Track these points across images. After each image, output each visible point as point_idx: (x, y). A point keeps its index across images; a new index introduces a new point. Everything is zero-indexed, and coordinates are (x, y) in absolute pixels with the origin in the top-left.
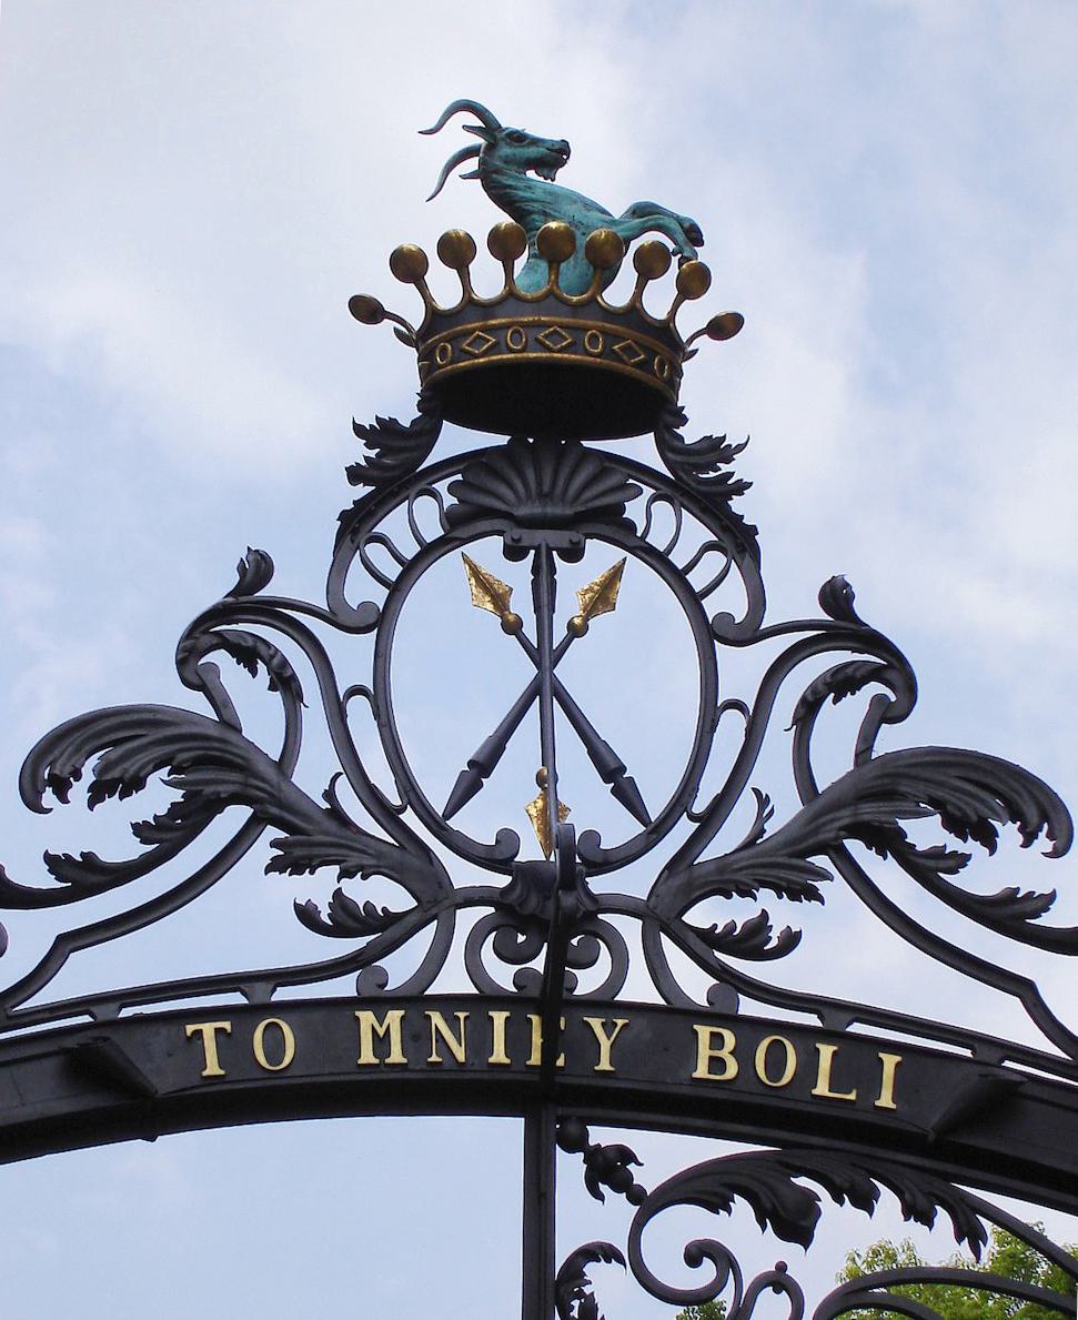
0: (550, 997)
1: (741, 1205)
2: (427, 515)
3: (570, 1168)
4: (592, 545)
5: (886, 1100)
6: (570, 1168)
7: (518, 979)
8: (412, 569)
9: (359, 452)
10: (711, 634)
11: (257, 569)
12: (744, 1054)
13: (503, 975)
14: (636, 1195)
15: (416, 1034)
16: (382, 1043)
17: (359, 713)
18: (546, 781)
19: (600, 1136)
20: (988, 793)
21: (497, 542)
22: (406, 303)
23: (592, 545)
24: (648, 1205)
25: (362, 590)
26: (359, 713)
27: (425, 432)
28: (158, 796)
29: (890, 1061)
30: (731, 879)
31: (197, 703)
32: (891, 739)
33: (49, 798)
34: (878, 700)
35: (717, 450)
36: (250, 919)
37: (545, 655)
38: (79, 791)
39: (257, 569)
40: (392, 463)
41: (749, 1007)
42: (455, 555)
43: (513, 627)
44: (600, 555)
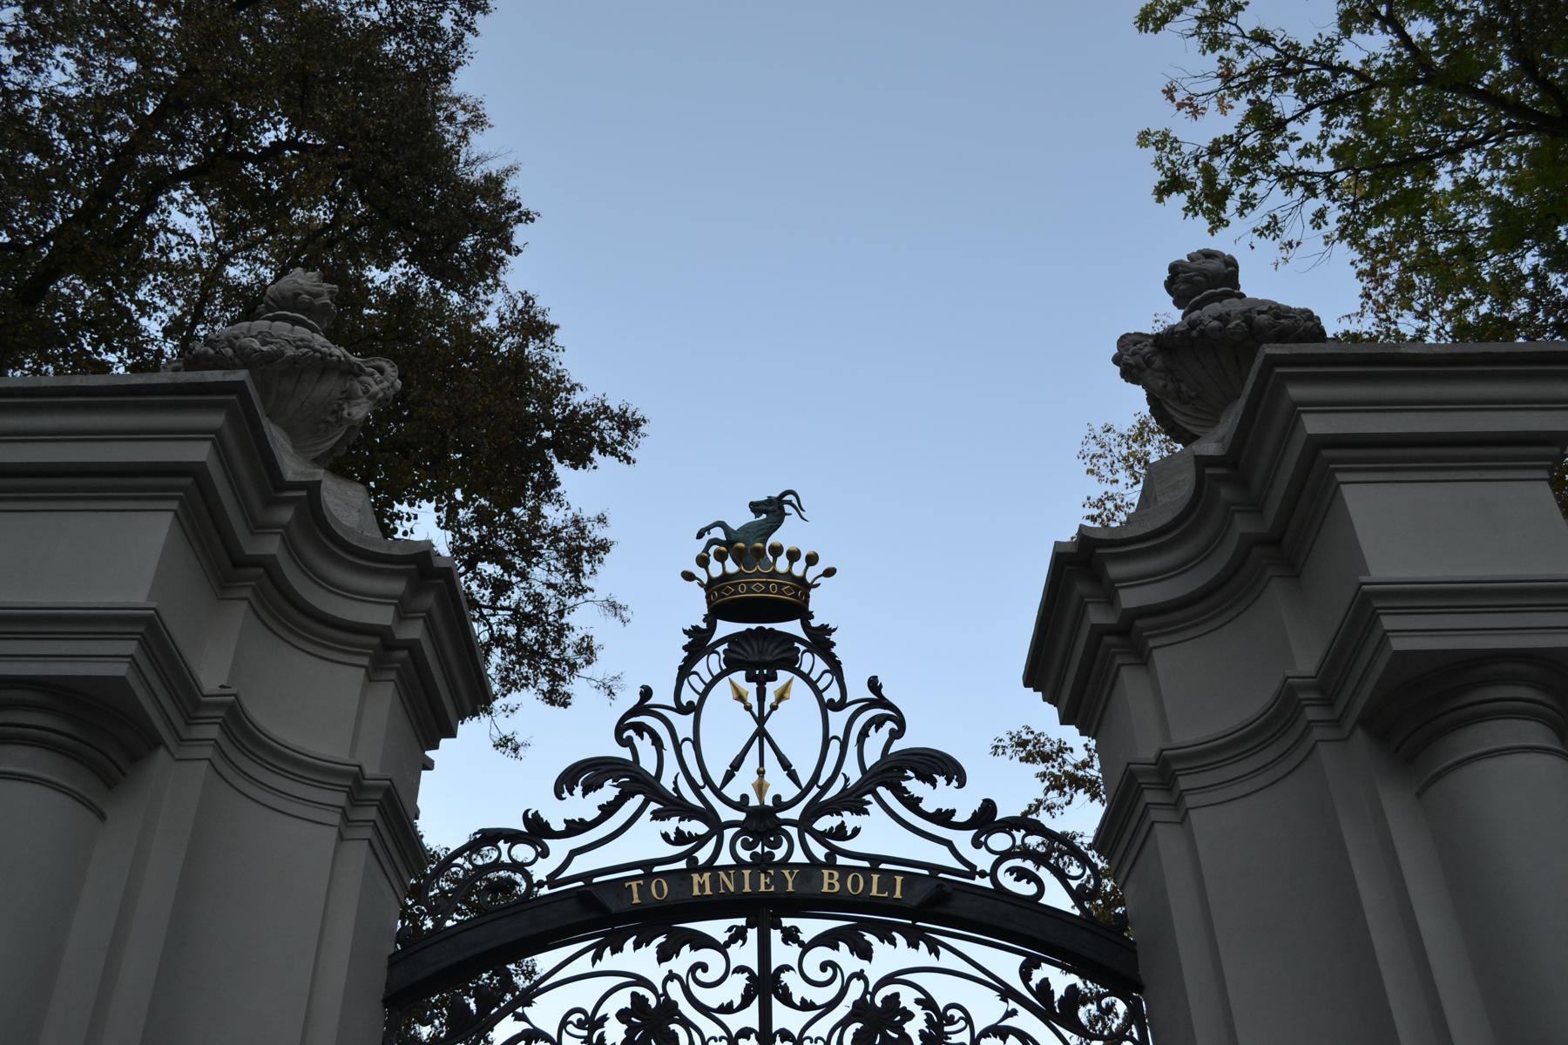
0: (762, 863)
1: (842, 945)
2: (714, 663)
3: (776, 935)
4: (779, 672)
5: (898, 895)
6: (776, 935)
7: (753, 856)
8: (709, 687)
9: (686, 640)
10: (827, 706)
11: (646, 693)
12: (842, 881)
13: (745, 855)
14: (801, 944)
15: (715, 881)
16: (702, 886)
17: (687, 749)
18: (761, 773)
19: (787, 922)
21: (742, 674)
22: (701, 573)
23: (779, 672)
24: (806, 948)
25: (688, 696)
26: (687, 749)
27: (712, 628)
28: (609, 792)
29: (899, 879)
30: (834, 807)
31: (625, 753)
32: (897, 746)
33: (566, 794)
34: (892, 731)
35: (825, 630)
36: (647, 839)
37: (761, 720)
38: (578, 790)
39: (646, 693)
40: (698, 643)
41: (841, 861)
42: (726, 679)
43: (748, 708)
44: (783, 676)
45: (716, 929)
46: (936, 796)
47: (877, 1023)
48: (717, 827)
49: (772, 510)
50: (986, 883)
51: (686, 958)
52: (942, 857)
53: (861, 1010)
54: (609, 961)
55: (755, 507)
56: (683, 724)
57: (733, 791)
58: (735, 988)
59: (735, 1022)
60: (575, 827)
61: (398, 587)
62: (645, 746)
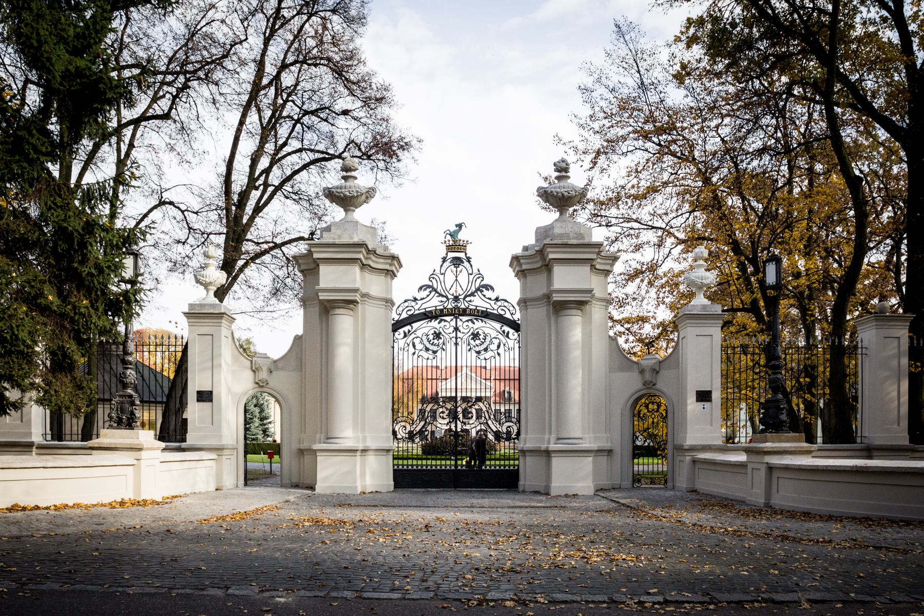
0: (456, 308)
10: (469, 274)
20: (488, 287)
25: (443, 271)
30: (470, 295)
31: (430, 284)
36: (434, 303)
40: (444, 260)
41: (471, 307)
45: (448, 318)
46: (488, 293)
47: (475, 336)
48: (448, 299)
49: (460, 226)
50: (495, 312)
51: (443, 323)
52: (488, 306)
53: (473, 334)
54: (430, 324)
55: (457, 226)
56: (442, 277)
57: (451, 292)
58: (452, 329)
59: (451, 335)
60: (422, 299)
61: (390, 261)
62: (434, 281)
